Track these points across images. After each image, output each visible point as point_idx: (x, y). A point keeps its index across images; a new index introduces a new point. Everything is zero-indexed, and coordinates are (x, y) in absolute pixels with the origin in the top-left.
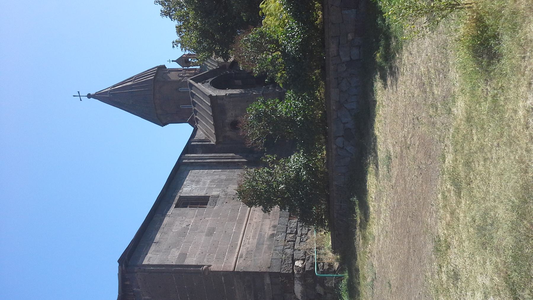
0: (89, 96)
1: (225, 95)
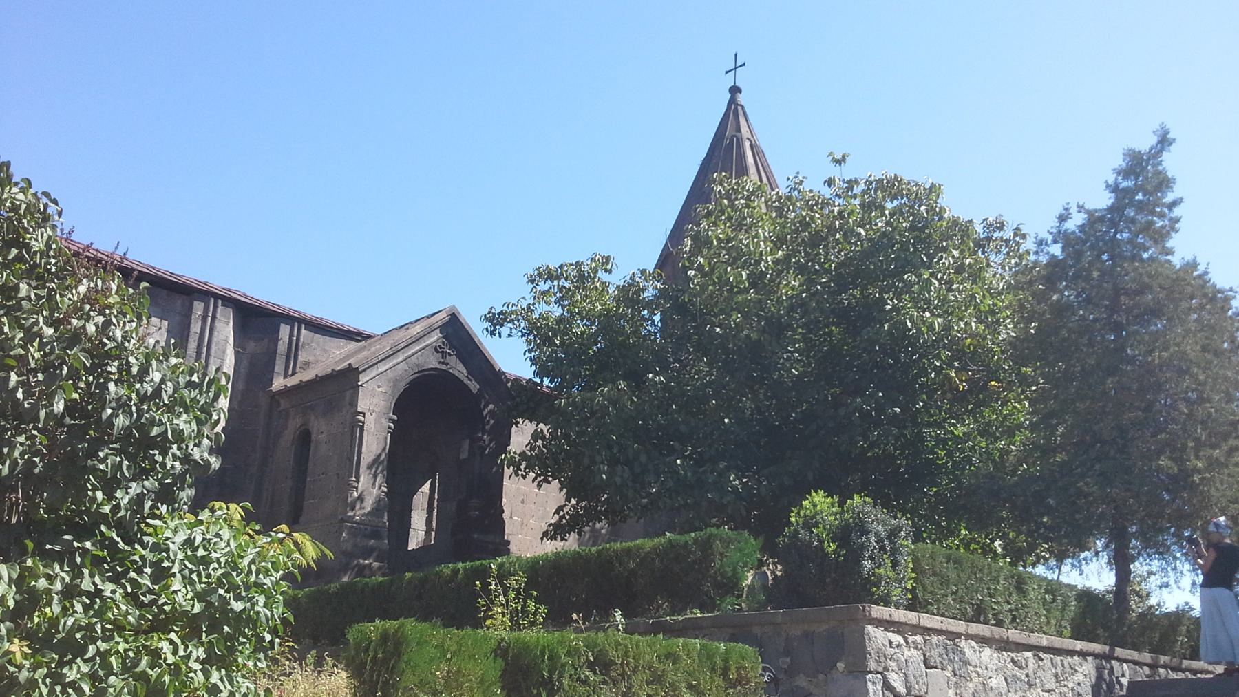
0: (735, 90)
1: (359, 410)
